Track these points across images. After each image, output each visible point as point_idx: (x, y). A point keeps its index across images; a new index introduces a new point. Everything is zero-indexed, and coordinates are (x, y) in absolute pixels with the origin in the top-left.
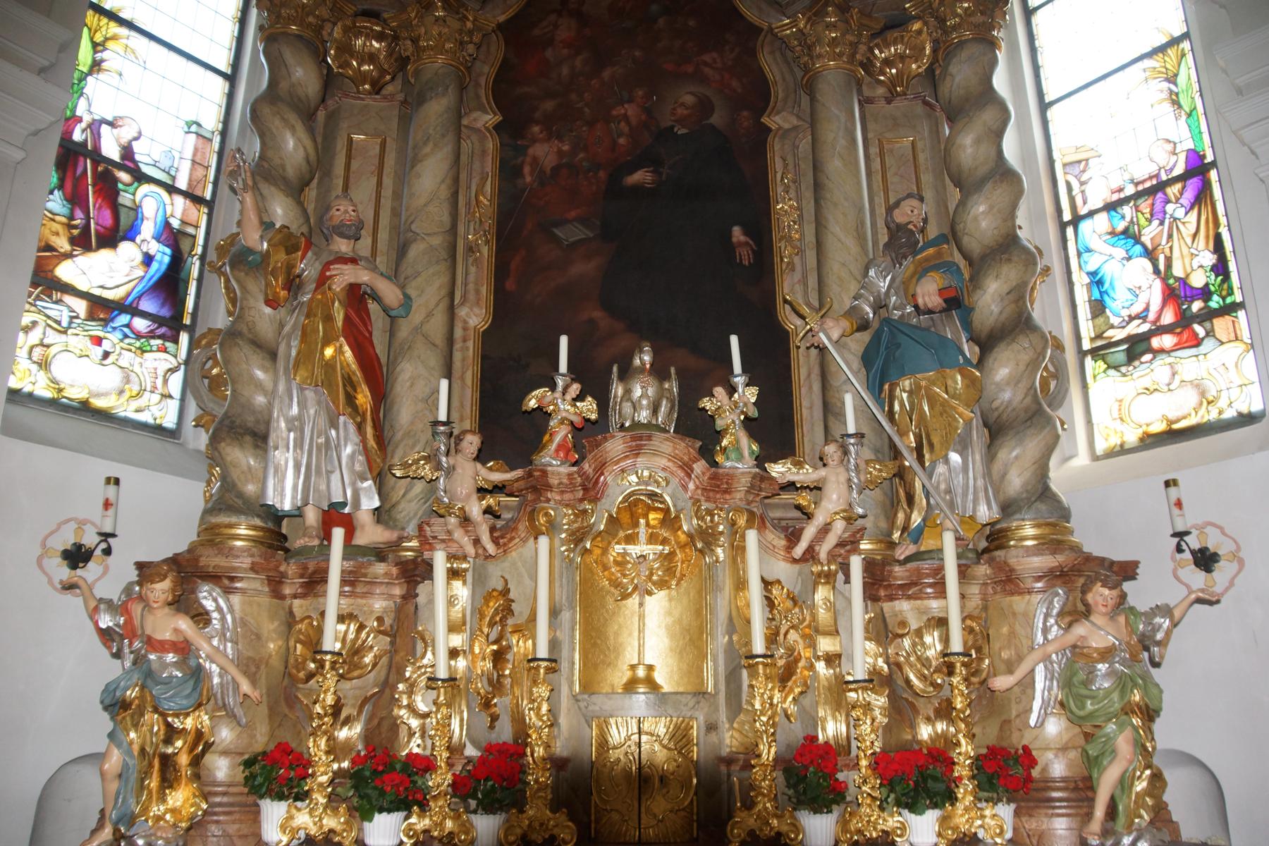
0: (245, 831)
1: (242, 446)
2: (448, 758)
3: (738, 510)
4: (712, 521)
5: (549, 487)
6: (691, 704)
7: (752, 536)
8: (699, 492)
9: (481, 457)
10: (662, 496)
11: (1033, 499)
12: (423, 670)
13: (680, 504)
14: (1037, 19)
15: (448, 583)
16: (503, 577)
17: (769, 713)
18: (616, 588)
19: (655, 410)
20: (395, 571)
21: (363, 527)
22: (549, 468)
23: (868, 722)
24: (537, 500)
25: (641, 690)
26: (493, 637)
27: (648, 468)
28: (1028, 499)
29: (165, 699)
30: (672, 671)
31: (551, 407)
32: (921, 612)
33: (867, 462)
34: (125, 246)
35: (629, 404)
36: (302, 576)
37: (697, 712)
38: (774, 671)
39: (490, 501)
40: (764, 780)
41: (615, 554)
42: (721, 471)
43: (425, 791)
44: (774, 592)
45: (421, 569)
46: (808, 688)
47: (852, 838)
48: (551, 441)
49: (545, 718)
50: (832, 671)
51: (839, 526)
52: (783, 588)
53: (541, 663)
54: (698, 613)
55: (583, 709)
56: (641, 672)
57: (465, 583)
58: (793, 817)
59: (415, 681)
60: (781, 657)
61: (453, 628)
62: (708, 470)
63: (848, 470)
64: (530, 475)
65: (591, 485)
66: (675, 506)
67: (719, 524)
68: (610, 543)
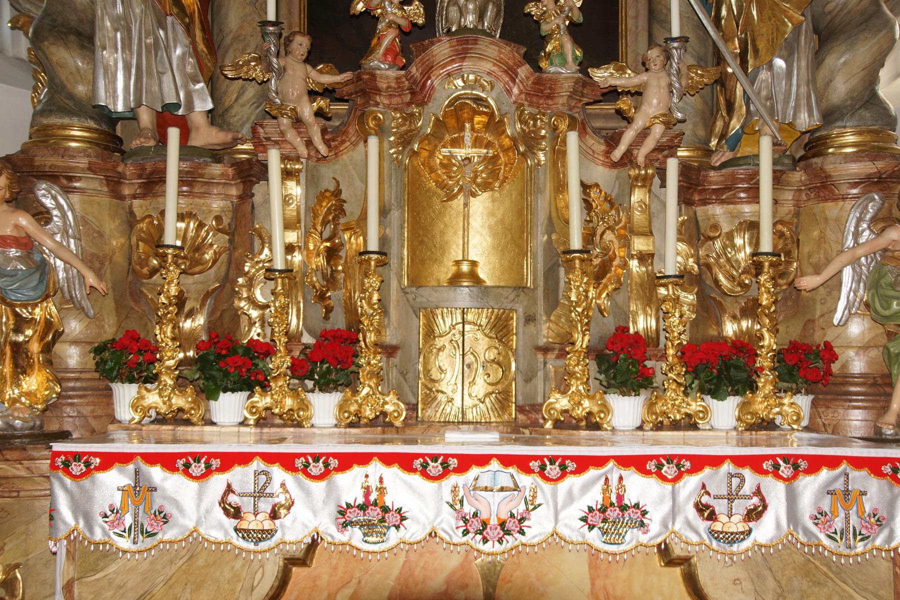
0: (99, 412)
1: (67, 46)
2: (287, 343)
3: (560, 115)
4: (535, 125)
5: (378, 91)
6: (512, 297)
7: (573, 138)
8: (523, 96)
9: (311, 59)
10: (486, 101)
11: (857, 107)
12: (261, 265)
13: (505, 108)
15: (283, 183)
16: (334, 178)
17: (584, 304)
18: (442, 189)
19: (481, 17)
20: (230, 171)
21: (198, 129)
22: (378, 72)
23: (677, 315)
24: (366, 104)
25: (465, 284)
26: (326, 234)
27: (473, 73)
28: (852, 106)
29: (11, 290)
30: (494, 268)
31: (379, 11)
32: (733, 216)
33: (689, 68)
35: (456, 8)
36: (140, 177)
37: (517, 305)
38: (590, 269)
39: (321, 103)
40: (578, 365)
41: (441, 157)
42: (544, 76)
43: (266, 372)
44: (592, 195)
45: (256, 169)
46: (621, 285)
47: (657, 419)
48: (379, 44)
49: (376, 306)
50: (644, 269)
51: (658, 130)
52: (601, 191)
53: (372, 256)
54: (520, 213)
55: (412, 301)
56: (465, 268)
57: (298, 183)
58: (602, 398)
59: (254, 275)
60: (597, 257)
61: (288, 226)
62: (532, 74)
63: (669, 75)
64: (359, 78)
65: (418, 89)
66: (499, 110)
67: (541, 128)
68: (436, 146)
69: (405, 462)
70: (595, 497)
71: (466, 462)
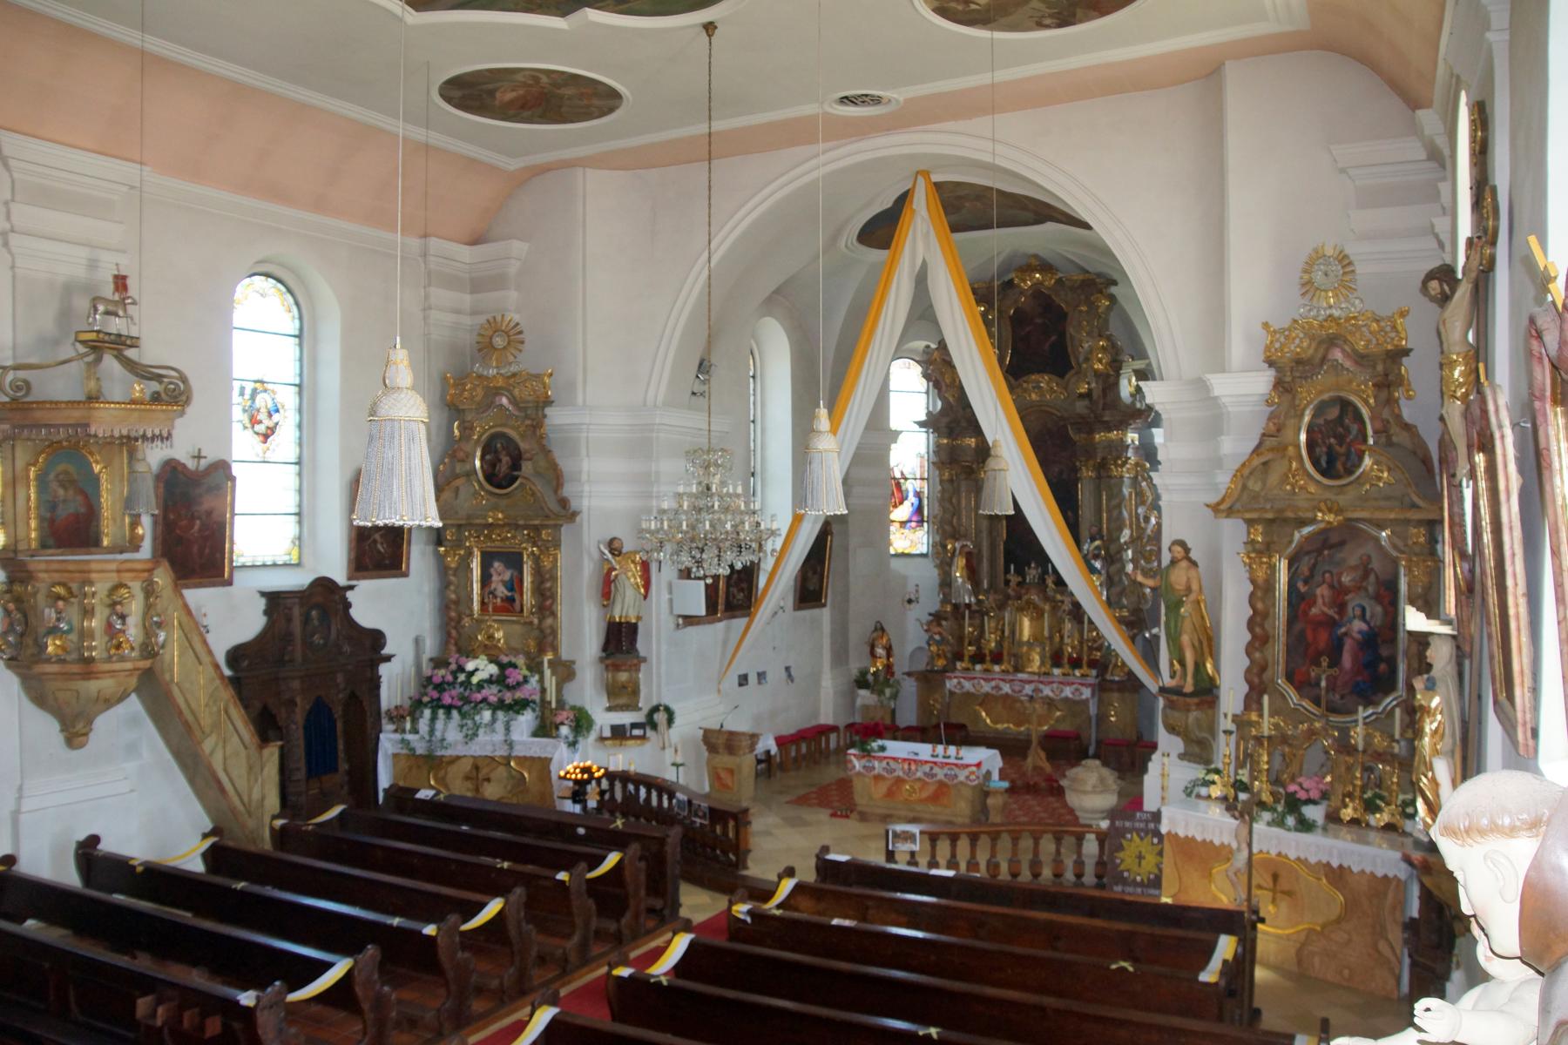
34: (906, 502)
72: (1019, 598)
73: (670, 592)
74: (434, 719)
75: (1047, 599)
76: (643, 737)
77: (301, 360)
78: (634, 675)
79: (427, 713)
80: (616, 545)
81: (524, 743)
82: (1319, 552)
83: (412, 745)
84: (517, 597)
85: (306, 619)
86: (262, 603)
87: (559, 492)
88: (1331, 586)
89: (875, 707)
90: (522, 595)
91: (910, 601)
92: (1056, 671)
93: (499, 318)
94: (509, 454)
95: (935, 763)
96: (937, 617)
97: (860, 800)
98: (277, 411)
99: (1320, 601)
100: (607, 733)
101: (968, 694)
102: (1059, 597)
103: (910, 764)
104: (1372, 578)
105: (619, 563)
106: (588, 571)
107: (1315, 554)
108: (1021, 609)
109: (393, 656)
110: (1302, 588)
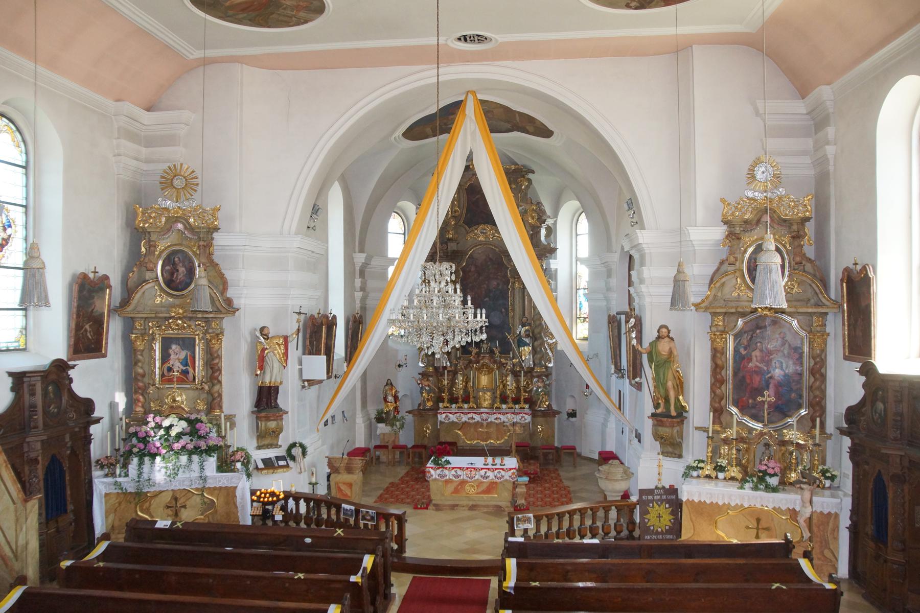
14: (578, 237)
69: (475, 413)
70: (496, 417)
71: (482, 413)
72: (478, 362)
73: (300, 363)
74: (141, 463)
75: (495, 362)
76: (287, 466)
77: (27, 186)
78: (280, 423)
79: (135, 460)
80: (265, 332)
81: (214, 478)
82: (754, 331)
83: (124, 486)
84: (191, 370)
85: (45, 394)
86: (9, 381)
87: (225, 294)
88: (761, 351)
89: (390, 434)
90: (194, 369)
91: (399, 366)
92: (504, 406)
93: (178, 167)
94: (184, 266)
95: (488, 469)
96: (424, 375)
97: (436, 498)
98: (10, 226)
99: (754, 359)
100: (261, 465)
101: (453, 422)
102: (503, 361)
103: (471, 471)
104: (787, 345)
105: (268, 344)
106: (244, 349)
107: (751, 333)
108: (478, 369)
109: (102, 418)
110: (743, 352)
